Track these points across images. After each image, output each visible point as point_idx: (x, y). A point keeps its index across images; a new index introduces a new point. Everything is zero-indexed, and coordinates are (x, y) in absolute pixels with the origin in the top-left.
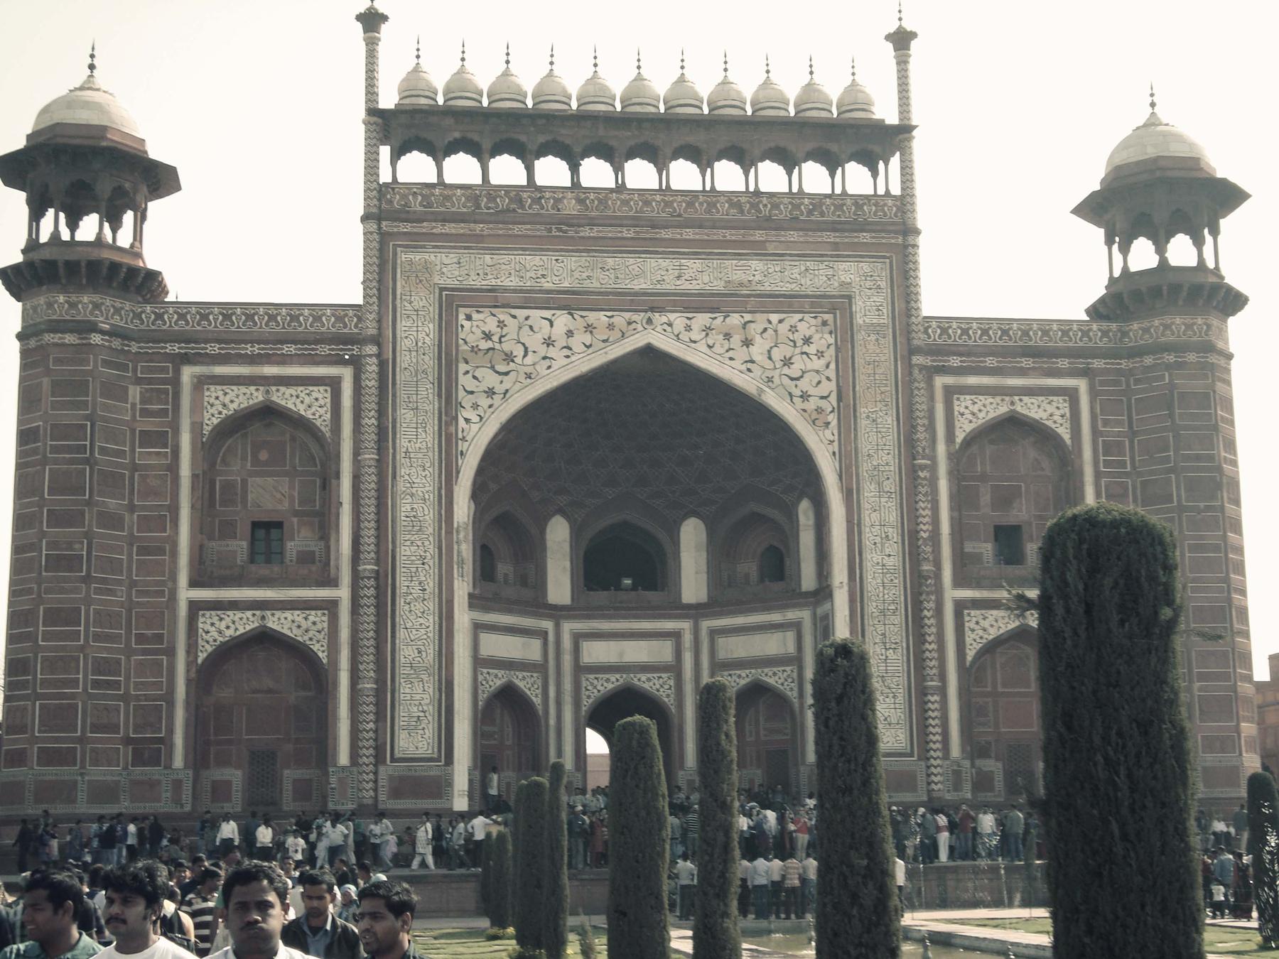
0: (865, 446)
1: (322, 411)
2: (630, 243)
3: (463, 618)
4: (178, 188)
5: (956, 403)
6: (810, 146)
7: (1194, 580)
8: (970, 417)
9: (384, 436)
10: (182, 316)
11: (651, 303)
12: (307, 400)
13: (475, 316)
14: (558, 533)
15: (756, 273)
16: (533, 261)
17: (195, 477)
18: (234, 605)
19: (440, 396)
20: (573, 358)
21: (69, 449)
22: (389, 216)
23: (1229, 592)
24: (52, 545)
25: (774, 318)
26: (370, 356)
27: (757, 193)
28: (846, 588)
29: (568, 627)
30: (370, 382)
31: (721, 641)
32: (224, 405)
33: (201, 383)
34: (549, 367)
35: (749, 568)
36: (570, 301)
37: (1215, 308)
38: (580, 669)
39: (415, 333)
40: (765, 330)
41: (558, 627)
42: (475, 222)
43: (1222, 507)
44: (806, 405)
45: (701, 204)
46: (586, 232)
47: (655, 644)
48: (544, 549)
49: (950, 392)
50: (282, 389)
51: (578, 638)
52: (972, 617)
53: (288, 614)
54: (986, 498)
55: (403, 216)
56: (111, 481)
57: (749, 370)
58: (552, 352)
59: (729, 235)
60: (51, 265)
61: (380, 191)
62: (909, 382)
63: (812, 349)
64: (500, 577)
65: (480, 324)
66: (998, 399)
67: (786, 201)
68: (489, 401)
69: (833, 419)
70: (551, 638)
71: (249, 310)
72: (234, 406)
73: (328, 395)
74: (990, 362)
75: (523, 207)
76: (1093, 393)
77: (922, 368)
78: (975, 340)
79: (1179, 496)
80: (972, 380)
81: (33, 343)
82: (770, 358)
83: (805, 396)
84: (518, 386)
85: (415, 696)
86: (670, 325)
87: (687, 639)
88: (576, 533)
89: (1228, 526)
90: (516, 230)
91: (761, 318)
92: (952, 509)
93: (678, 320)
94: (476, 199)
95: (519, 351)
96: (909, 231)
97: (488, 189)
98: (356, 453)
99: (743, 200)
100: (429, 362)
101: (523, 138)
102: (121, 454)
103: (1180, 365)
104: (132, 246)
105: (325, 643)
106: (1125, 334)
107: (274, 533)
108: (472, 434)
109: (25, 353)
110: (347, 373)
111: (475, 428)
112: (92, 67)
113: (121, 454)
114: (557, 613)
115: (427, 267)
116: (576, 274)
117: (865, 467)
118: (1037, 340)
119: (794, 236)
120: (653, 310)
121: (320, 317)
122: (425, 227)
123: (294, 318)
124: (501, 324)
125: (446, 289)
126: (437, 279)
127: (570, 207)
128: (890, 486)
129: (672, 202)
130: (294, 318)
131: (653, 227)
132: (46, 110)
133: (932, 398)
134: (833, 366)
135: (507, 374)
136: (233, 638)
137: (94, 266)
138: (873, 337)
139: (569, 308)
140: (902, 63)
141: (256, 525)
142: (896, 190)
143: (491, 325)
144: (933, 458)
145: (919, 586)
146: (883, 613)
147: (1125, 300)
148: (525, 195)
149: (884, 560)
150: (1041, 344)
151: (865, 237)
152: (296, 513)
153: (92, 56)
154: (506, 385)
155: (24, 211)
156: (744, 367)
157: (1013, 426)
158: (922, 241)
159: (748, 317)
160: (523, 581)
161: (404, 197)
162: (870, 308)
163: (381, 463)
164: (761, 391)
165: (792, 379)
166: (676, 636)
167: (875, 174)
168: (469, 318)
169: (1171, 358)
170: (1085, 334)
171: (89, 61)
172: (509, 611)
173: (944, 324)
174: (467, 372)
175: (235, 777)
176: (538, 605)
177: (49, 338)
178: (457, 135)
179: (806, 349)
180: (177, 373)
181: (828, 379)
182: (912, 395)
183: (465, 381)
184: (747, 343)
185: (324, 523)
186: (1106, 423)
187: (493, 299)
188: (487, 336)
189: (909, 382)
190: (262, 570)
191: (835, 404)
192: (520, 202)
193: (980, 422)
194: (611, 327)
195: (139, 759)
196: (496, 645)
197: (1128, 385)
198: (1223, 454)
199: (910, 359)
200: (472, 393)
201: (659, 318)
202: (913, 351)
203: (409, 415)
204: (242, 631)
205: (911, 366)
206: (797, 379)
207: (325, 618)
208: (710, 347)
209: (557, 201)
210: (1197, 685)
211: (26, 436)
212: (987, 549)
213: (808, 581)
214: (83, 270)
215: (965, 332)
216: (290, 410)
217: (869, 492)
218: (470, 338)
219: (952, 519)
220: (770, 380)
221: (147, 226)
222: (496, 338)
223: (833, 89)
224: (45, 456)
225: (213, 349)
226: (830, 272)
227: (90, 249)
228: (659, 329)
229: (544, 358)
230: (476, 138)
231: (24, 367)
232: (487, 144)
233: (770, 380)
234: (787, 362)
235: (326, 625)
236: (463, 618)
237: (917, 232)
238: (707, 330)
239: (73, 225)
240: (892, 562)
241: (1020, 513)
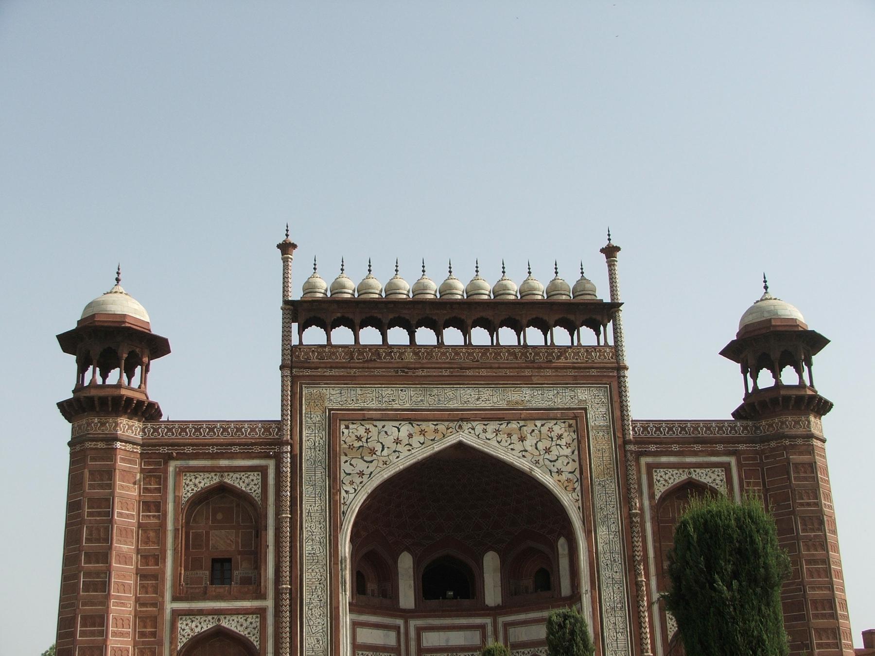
0: (598, 503)
1: (255, 488)
2: (446, 378)
3: (346, 619)
4: (169, 352)
5: (655, 474)
6: (557, 317)
7: (810, 583)
8: (663, 482)
10: (170, 430)
11: (460, 417)
12: (247, 481)
13: (351, 426)
14: (406, 562)
16: (387, 392)
17: (176, 530)
18: (201, 612)
19: (329, 477)
20: (413, 451)
21: (99, 514)
22: (298, 367)
23: (833, 591)
24: (87, 574)
25: (539, 423)
26: (286, 452)
27: (526, 346)
28: (589, 594)
29: (413, 623)
31: (511, 630)
32: (195, 485)
34: (398, 457)
36: (411, 417)
37: (812, 410)
40: (533, 431)
41: (406, 623)
42: (350, 368)
43: (825, 535)
44: (560, 478)
45: (491, 354)
46: (420, 373)
47: (468, 633)
48: (397, 574)
49: (650, 467)
50: (231, 474)
51: (419, 630)
53: (234, 617)
55: (307, 365)
56: (124, 532)
57: (524, 456)
58: (399, 448)
59: (509, 373)
60: (91, 399)
61: (291, 351)
63: (563, 442)
64: (369, 592)
65: (355, 431)
66: (681, 471)
67: (543, 350)
68: (360, 480)
69: (577, 485)
70: (402, 630)
71: (211, 426)
72: (202, 485)
73: (260, 477)
74: (675, 448)
75: (380, 358)
77: (632, 452)
78: (665, 434)
79: (797, 529)
80: (664, 459)
81: (78, 448)
82: (537, 448)
83: (559, 472)
84: (379, 469)
86: (473, 429)
87: (490, 629)
89: (829, 547)
90: (376, 372)
91: (528, 422)
92: (654, 541)
93: (479, 428)
94: (352, 353)
95: (379, 447)
96: (620, 368)
97: (358, 348)
98: (278, 513)
99: (517, 350)
100: (321, 456)
101: (379, 316)
102: (128, 516)
103: (793, 447)
104: (140, 387)
105: (258, 635)
106: (757, 428)
107: (226, 565)
108: (350, 500)
109: (72, 455)
110: (271, 464)
111: (351, 496)
112: (118, 280)
113: (128, 516)
114: (406, 614)
115: (321, 397)
116: (414, 399)
117: (599, 516)
118: (703, 434)
119: (549, 372)
120: (462, 420)
121: (255, 429)
122: (320, 372)
123: (239, 430)
124: (367, 431)
125: (333, 410)
126: (326, 404)
127: (409, 357)
128: (613, 528)
129: (473, 353)
130: (239, 430)
131: (461, 368)
132: (90, 306)
133: (639, 471)
134: (576, 452)
135: (371, 462)
136: (200, 634)
137: (117, 399)
138: (601, 434)
139: (410, 421)
140: (611, 265)
141: (214, 561)
142: (611, 342)
143: (361, 431)
144: (642, 509)
146: (613, 609)
147: (755, 406)
148: (381, 351)
149: (612, 574)
150: (705, 435)
151: (594, 372)
152: (240, 553)
153: (118, 273)
154: (371, 469)
155: (75, 366)
156: (520, 454)
158: (627, 373)
159: (522, 423)
160: (384, 594)
161: (306, 353)
162: (597, 415)
163: (293, 521)
164: (532, 469)
165: (551, 461)
166: (482, 627)
167: (598, 334)
168: (347, 427)
169: (787, 442)
170: (733, 428)
171: (116, 276)
172: (374, 614)
173: (646, 425)
174: (346, 461)
176: (394, 610)
177: (88, 445)
178: (339, 315)
179: (559, 442)
180: (166, 464)
181: (574, 460)
182: (627, 470)
183: (346, 467)
184: (522, 439)
185: (256, 558)
186: (748, 484)
187: (362, 417)
188: (359, 439)
191: (578, 476)
192: (379, 356)
193: (670, 486)
194: (436, 431)
196: (367, 636)
197: (761, 459)
198: (823, 502)
199: (625, 447)
200: (350, 474)
201: (466, 426)
202: (626, 442)
203: (311, 489)
204: (205, 628)
205: (625, 451)
206: (555, 461)
207: (258, 620)
208: (499, 442)
209: (401, 354)
210: (817, 651)
211: (73, 507)
213: (565, 589)
214: (110, 403)
215: (658, 429)
216: (236, 487)
218: (348, 440)
219: (655, 547)
220: (537, 462)
221: (149, 375)
222: (364, 440)
224: (83, 519)
225: (189, 450)
226: (572, 394)
227: (114, 390)
228: (466, 431)
229: (395, 451)
230: (351, 316)
231: (72, 463)
232: (357, 321)
233: (537, 462)
234: (548, 450)
235: (258, 624)
236: (346, 619)
237: (626, 368)
238: (497, 432)
239: (104, 376)
240: (617, 576)
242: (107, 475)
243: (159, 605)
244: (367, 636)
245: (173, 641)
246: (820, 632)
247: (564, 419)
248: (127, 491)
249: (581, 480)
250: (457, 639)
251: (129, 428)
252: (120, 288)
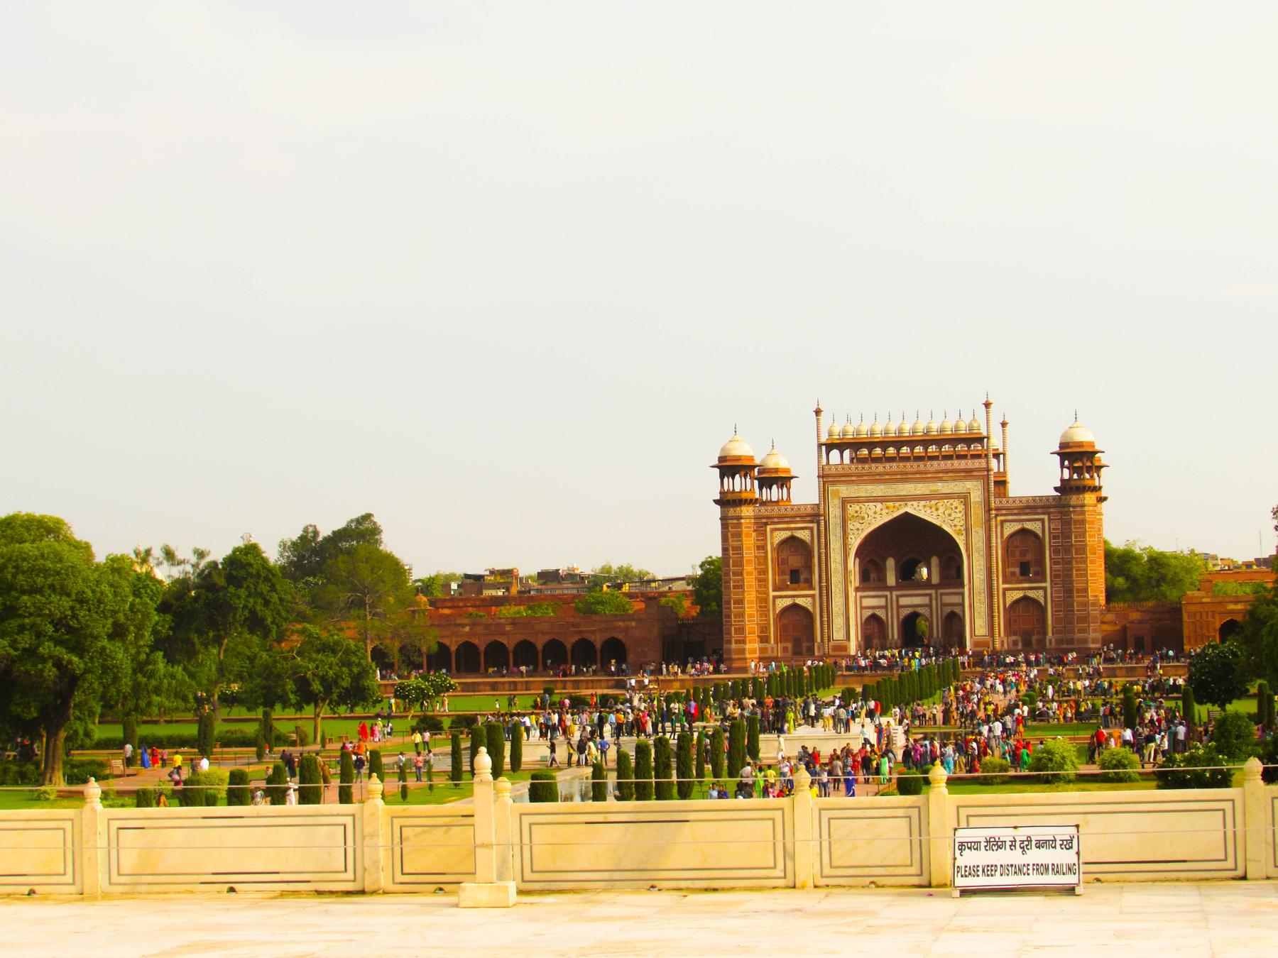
14: (890, 563)
15: (942, 487)
16: (870, 487)
18: (786, 597)
29: (895, 593)
30: (822, 528)
33: (773, 530)
35: (954, 572)
36: (882, 499)
38: (899, 607)
39: (834, 512)
49: (1002, 522)
51: (898, 597)
52: (1008, 593)
54: (1017, 553)
62: (988, 520)
76: (1050, 520)
85: (838, 622)
88: (897, 563)
93: (915, 503)
100: (839, 521)
110: (815, 526)
114: (891, 589)
132: (723, 450)
157: (1023, 531)
160: (879, 580)
166: (930, 595)
175: (789, 645)
183: (850, 526)
187: (857, 500)
189: (988, 520)
190: (795, 586)
195: (761, 642)
196: (866, 602)
212: (1017, 570)
217: (975, 555)
241: (1029, 557)
242: (738, 535)
243: (767, 594)
244: (866, 602)
245: (774, 609)
246: (1080, 604)
247: (959, 498)
248: (749, 541)
249: (966, 529)
250: (917, 601)
251: (747, 511)
252: (737, 437)
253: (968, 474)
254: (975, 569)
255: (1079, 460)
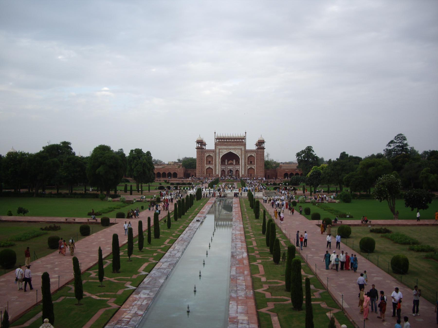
9: (216, 157)
11: (230, 149)
14: (226, 160)
15: (236, 147)
36: (226, 149)
39: (217, 151)
85: (217, 171)
145: (245, 165)
149: (243, 164)
157: (251, 156)
176: (225, 165)
187: (222, 149)
196: (222, 167)
223: (242, 135)
244: (222, 167)
250: (231, 167)
253: (242, 145)
254: (242, 162)
255: (260, 143)
